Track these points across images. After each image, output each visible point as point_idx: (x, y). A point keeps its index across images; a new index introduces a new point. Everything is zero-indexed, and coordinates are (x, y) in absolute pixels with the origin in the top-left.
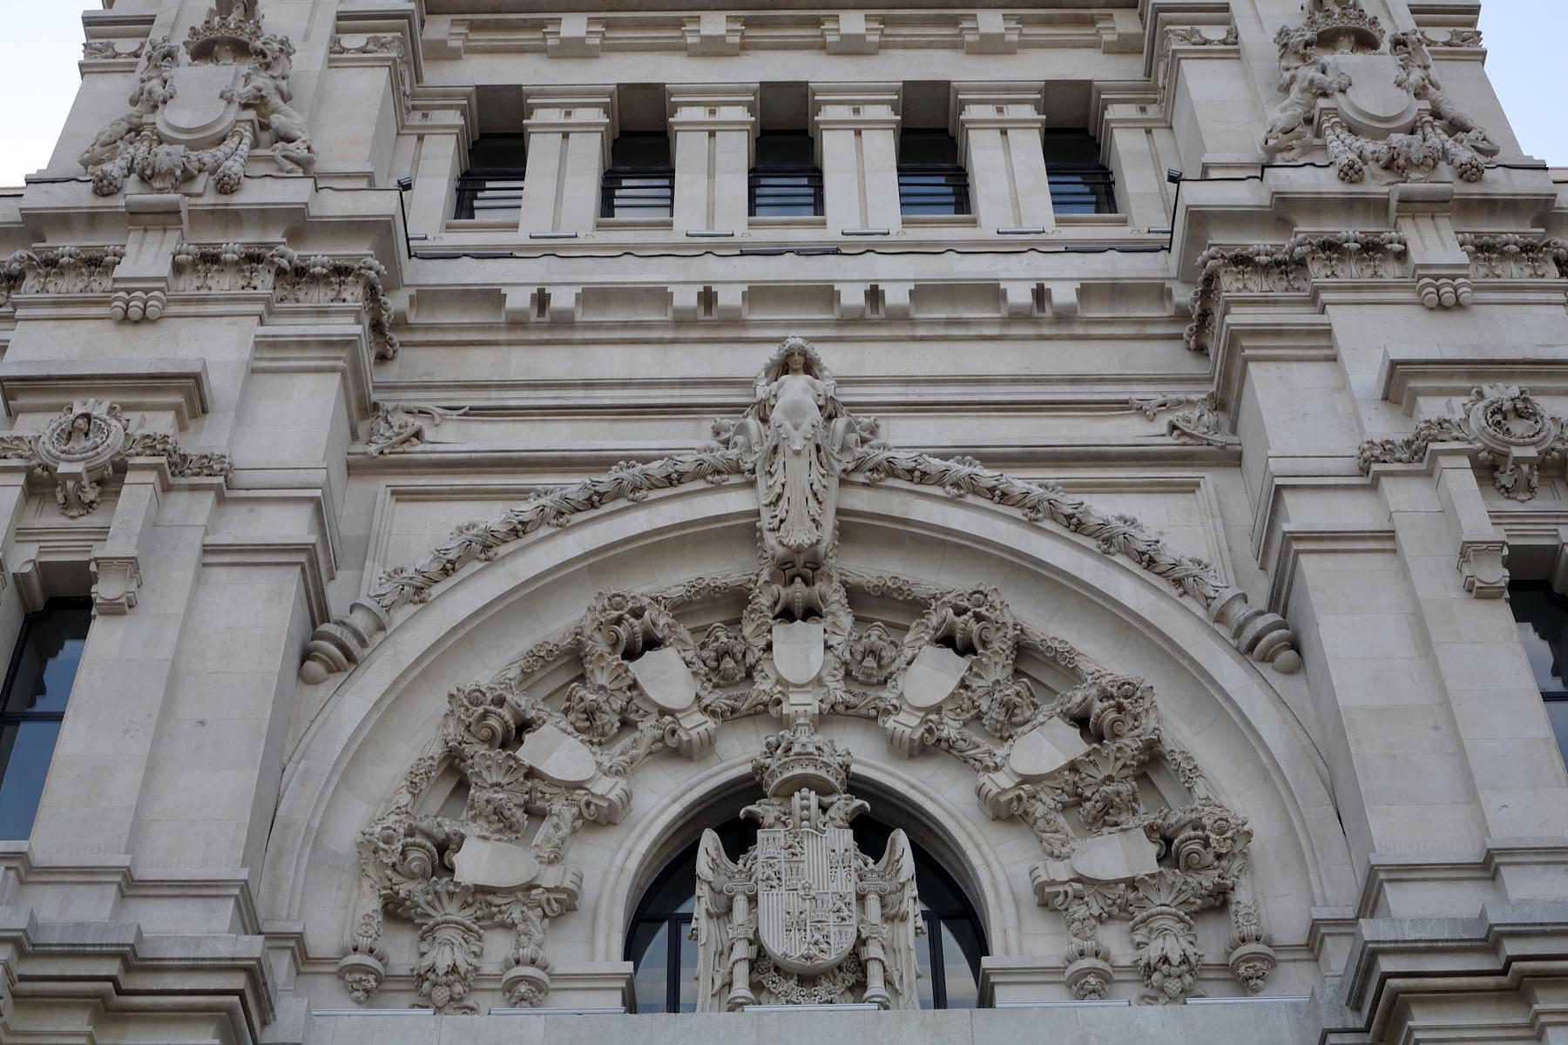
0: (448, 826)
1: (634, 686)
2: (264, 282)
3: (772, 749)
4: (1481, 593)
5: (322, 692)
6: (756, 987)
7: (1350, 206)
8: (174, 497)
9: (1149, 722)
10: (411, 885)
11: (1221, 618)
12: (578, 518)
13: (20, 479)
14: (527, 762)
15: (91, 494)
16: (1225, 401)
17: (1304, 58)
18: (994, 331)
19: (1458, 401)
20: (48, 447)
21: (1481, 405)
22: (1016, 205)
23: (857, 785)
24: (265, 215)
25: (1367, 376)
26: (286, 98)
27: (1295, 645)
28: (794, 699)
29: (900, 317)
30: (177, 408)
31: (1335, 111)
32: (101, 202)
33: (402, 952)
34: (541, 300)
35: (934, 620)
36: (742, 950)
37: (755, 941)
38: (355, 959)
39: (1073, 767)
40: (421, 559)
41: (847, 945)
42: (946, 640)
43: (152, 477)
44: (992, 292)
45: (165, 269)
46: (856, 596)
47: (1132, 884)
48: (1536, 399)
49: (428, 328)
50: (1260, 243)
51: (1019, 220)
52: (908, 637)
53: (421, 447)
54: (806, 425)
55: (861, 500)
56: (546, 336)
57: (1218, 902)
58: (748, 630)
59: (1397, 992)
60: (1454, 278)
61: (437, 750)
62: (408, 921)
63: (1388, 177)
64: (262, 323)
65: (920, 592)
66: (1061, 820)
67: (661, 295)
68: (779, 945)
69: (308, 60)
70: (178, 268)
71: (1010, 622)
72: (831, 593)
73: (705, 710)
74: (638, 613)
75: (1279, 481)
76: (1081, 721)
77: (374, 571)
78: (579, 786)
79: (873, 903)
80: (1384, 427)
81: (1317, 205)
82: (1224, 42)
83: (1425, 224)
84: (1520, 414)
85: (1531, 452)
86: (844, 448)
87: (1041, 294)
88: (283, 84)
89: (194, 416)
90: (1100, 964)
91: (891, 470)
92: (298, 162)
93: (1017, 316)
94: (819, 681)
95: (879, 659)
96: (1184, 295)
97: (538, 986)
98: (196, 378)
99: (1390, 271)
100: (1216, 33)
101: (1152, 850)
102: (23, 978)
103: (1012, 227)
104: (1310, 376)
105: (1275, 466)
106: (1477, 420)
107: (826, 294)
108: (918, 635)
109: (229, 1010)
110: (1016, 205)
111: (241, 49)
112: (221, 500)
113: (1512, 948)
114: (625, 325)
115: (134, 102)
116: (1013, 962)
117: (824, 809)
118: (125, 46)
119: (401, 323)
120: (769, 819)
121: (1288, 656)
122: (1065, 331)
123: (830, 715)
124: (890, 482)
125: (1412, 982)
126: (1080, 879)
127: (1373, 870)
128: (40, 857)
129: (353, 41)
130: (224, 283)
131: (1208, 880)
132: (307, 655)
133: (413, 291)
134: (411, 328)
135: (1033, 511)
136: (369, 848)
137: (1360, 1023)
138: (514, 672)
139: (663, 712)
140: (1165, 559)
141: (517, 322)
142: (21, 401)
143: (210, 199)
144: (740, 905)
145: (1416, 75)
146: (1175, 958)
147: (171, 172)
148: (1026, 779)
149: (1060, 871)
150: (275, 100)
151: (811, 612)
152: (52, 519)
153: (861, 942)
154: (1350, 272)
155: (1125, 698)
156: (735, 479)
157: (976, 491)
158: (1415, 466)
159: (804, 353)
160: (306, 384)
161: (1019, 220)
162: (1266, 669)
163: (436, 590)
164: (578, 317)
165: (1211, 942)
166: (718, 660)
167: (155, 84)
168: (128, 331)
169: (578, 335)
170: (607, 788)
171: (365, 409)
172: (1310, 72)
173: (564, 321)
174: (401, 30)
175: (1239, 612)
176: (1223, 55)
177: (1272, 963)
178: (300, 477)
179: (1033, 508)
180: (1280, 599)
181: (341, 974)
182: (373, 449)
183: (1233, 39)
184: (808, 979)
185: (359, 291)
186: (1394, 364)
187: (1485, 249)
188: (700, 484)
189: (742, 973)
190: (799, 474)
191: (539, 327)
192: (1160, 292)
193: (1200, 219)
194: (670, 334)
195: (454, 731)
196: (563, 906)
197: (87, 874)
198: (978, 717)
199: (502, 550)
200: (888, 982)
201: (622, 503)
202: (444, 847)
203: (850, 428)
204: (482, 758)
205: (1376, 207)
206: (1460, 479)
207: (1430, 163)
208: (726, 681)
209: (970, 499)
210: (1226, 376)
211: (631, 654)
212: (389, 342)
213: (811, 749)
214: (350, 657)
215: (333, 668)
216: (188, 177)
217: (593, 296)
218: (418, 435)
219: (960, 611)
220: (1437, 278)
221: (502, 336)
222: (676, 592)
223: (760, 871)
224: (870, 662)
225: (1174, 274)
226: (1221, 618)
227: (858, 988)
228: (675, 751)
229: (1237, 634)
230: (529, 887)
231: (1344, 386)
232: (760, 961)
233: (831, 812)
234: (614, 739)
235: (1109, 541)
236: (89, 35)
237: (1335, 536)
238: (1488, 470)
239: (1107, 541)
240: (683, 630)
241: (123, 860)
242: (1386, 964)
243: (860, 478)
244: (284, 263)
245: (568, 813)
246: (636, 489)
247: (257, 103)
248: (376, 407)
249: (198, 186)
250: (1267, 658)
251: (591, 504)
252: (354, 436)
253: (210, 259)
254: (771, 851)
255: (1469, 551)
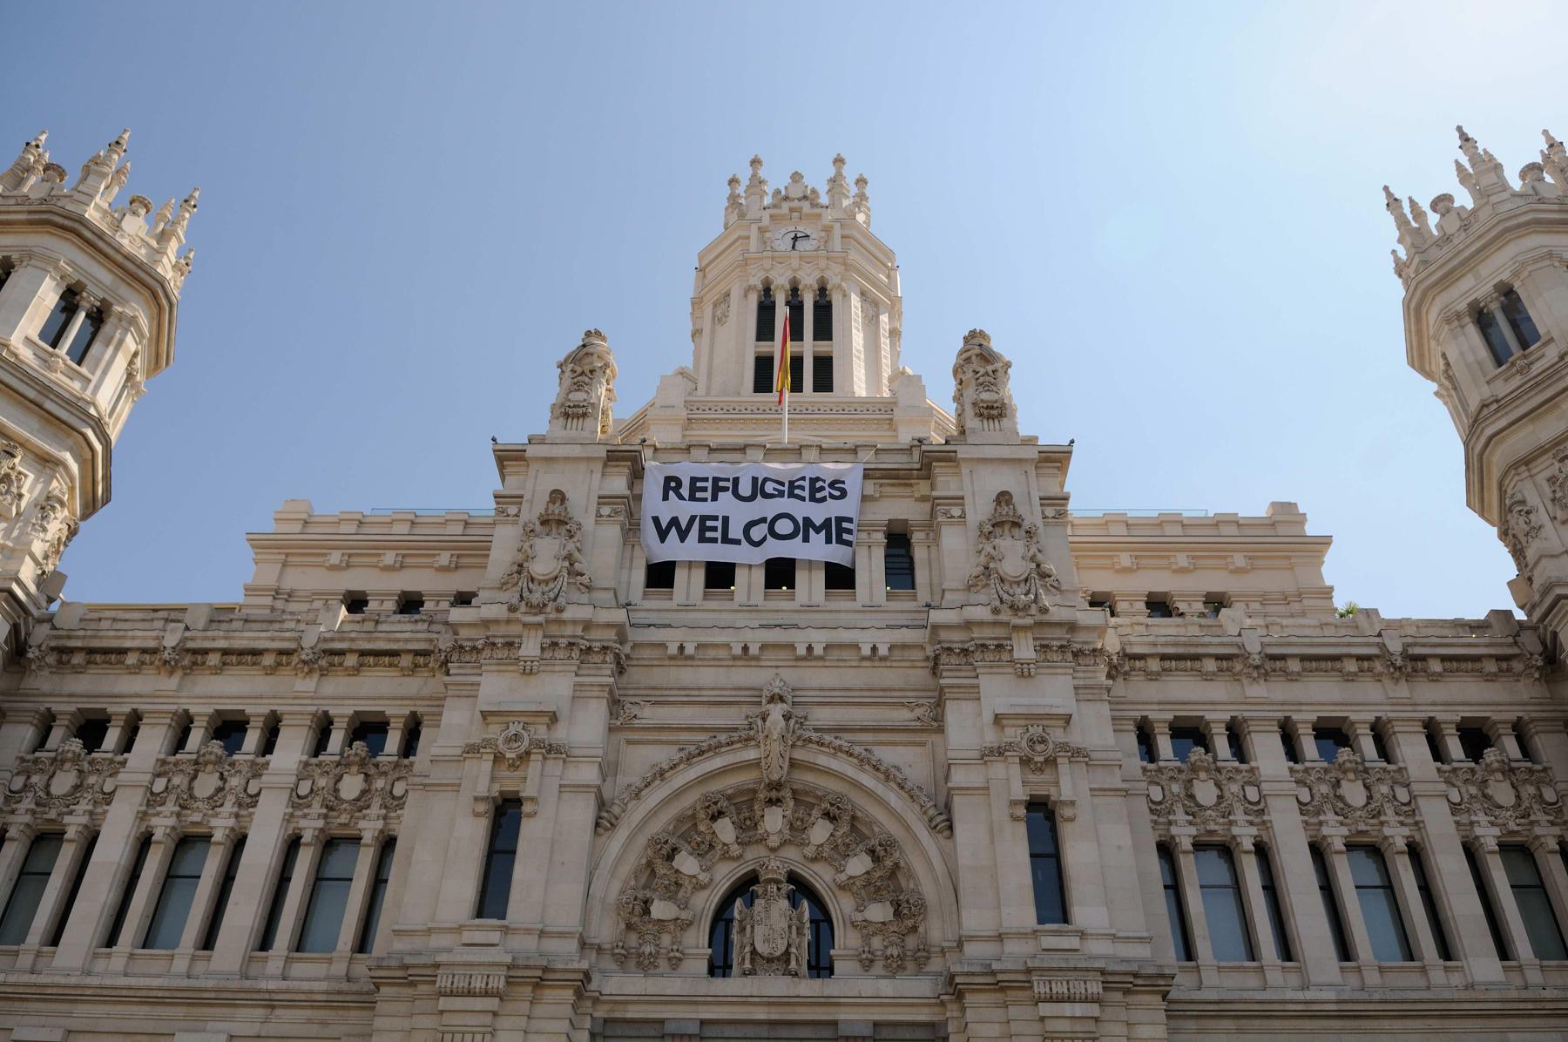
0: (648, 894)
1: (714, 832)
2: (576, 653)
3: (761, 866)
4: (1015, 819)
5: (603, 839)
6: (752, 961)
7: (995, 624)
8: (548, 762)
9: (897, 855)
10: (636, 919)
11: (925, 813)
12: (695, 760)
13: (492, 757)
14: (676, 867)
15: (518, 763)
16: (939, 704)
17: (988, 539)
18: (854, 664)
19: (1020, 731)
20: (502, 747)
21: (1028, 734)
22: (871, 588)
23: (793, 878)
24: (575, 622)
25: (988, 717)
26: (579, 550)
27: (951, 828)
28: (771, 838)
29: (821, 658)
30: (548, 725)
31: (996, 569)
32: (513, 615)
33: (633, 939)
34: (681, 648)
35: (823, 806)
36: (747, 949)
37: (752, 944)
38: (617, 951)
39: (867, 873)
40: (639, 783)
41: (784, 949)
42: (827, 815)
43: (540, 757)
44: (856, 647)
45: (538, 652)
46: (794, 792)
47: (883, 923)
48: (1048, 730)
49: (638, 659)
50: (956, 637)
51: (871, 601)
52: (814, 812)
53: (637, 721)
54: (779, 729)
55: (799, 755)
56: (684, 663)
57: (914, 929)
58: (756, 807)
59: (960, 990)
60: (1028, 664)
61: (644, 861)
62: (634, 929)
63: (1010, 613)
64: (577, 675)
65: (819, 793)
66: (863, 892)
67: (727, 646)
68: (762, 948)
69: (588, 522)
70: (543, 649)
71: (850, 807)
72: (786, 793)
73: (738, 844)
74: (715, 803)
75: (950, 761)
76: (872, 852)
77: (622, 780)
78: (694, 877)
79: (794, 928)
80: (991, 738)
81: (981, 624)
82: (960, 517)
83: (1022, 634)
84: (1040, 742)
85: (1041, 759)
86: (794, 732)
87: (874, 649)
88: (578, 545)
89: (553, 723)
90: (870, 956)
91: (810, 741)
92: (587, 587)
93: (864, 658)
94: (780, 831)
95: (802, 821)
96: (929, 652)
97: (680, 960)
98: (554, 713)
99: (1006, 657)
100: (956, 511)
101: (892, 910)
102: (510, 977)
103: (869, 603)
104: (968, 707)
105: (951, 754)
106: (1024, 744)
107: (791, 647)
108: (816, 813)
109: (578, 987)
110: (871, 588)
111: (561, 522)
112: (564, 761)
113: (1000, 977)
114: (714, 659)
115: (519, 550)
116: (841, 952)
117: (779, 889)
118: (512, 510)
119: (628, 657)
120: (760, 892)
121: (947, 833)
122: (883, 664)
123: (784, 843)
124: (810, 745)
125: (965, 987)
126: (865, 921)
127: (960, 937)
128: (513, 926)
129: (606, 510)
130: (560, 654)
131: (910, 923)
132: (597, 825)
133: (632, 644)
134: (632, 659)
135: (863, 762)
136: (620, 906)
137: (952, 992)
138: (671, 827)
139: (724, 844)
140: (909, 785)
141: (672, 658)
142: (490, 719)
143: (553, 616)
144: (748, 927)
145: (1033, 549)
146: (895, 955)
147: (538, 605)
148: (851, 877)
149: (859, 917)
150: (576, 554)
151: (779, 800)
152: (504, 772)
153: (789, 945)
154: (990, 656)
155: (889, 844)
156: (753, 743)
157: (841, 751)
158: (1000, 758)
159: (779, 695)
160: (594, 704)
161: (871, 601)
162: (939, 836)
163: (643, 793)
164: (697, 657)
165: (911, 942)
166: (745, 820)
167: (526, 546)
168: (526, 678)
169: (696, 663)
170: (704, 877)
171: (615, 704)
172: (989, 548)
173: (691, 658)
174: (625, 504)
175: (932, 812)
176: (959, 524)
177: (928, 958)
178: (594, 752)
179: (862, 760)
180: (948, 807)
181: (613, 955)
182: (619, 723)
183: (963, 516)
184: (770, 960)
185: (612, 656)
186: (997, 715)
187: (1044, 648)
188: (739, 745)
189: (748, 956)
190: (776, 748)
191: (681, 659)
192: (922, 647)
193: (936, 628)
194: (731, 663)
195: (650, 852)
196: (685, 925)
197: (528, 931)
198: (837, 846)
199: (667, 775)
200: (797, 960)
201: (711, 753)
202: (647, 903)
203: (796, 722)
204: (661, 870)
205: (1007, 624)
206: (1016, 770)
207: (1027, 607)
208: (749, 829)
209: (839, 754)
210: (940, 696)
211: (714, 818)
212: (623, 668)
213: (775, 868)
214: (612, 824)
215: (606, 829)
216: (545, 605)
217: (699, 646)
218: (635, 716)
219: (832, 805)
220: (1022, 664)
221: (667, 663)
222: (729, 792)
223: (757, 918)
224: (799, 823)
225: (927, 640)
226: (925, 813)
227: (788, 961)
228: (726, 856)
229: (931, 820)
230: (677, 919)
231: (980, 715)
232: (754, 952)
233: (782, 891)
234: (707, 852)
235: (887, 775)
236: (498, 503)
237: (967, 789)
238: (1025, 762)
239: (887, 778)
240: (733, 808)
241: (540, 926)
242: (958, 980)
243: (799, 743)
244: (584, 647)
245: (689, 888)
246: (716, 748)
247: (569, 557)
248: (619, 701)
249: (548, 609)
250: (940, 832)
251: (699, 755)
252: (611, 714)
253: (555, 644)
254: (760, 909)
255: (1014, 803)
